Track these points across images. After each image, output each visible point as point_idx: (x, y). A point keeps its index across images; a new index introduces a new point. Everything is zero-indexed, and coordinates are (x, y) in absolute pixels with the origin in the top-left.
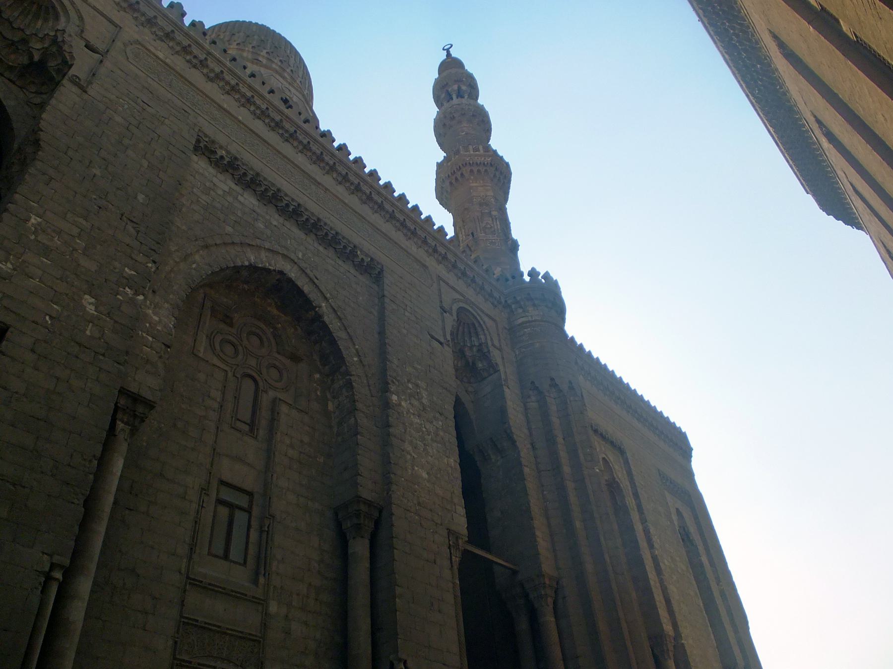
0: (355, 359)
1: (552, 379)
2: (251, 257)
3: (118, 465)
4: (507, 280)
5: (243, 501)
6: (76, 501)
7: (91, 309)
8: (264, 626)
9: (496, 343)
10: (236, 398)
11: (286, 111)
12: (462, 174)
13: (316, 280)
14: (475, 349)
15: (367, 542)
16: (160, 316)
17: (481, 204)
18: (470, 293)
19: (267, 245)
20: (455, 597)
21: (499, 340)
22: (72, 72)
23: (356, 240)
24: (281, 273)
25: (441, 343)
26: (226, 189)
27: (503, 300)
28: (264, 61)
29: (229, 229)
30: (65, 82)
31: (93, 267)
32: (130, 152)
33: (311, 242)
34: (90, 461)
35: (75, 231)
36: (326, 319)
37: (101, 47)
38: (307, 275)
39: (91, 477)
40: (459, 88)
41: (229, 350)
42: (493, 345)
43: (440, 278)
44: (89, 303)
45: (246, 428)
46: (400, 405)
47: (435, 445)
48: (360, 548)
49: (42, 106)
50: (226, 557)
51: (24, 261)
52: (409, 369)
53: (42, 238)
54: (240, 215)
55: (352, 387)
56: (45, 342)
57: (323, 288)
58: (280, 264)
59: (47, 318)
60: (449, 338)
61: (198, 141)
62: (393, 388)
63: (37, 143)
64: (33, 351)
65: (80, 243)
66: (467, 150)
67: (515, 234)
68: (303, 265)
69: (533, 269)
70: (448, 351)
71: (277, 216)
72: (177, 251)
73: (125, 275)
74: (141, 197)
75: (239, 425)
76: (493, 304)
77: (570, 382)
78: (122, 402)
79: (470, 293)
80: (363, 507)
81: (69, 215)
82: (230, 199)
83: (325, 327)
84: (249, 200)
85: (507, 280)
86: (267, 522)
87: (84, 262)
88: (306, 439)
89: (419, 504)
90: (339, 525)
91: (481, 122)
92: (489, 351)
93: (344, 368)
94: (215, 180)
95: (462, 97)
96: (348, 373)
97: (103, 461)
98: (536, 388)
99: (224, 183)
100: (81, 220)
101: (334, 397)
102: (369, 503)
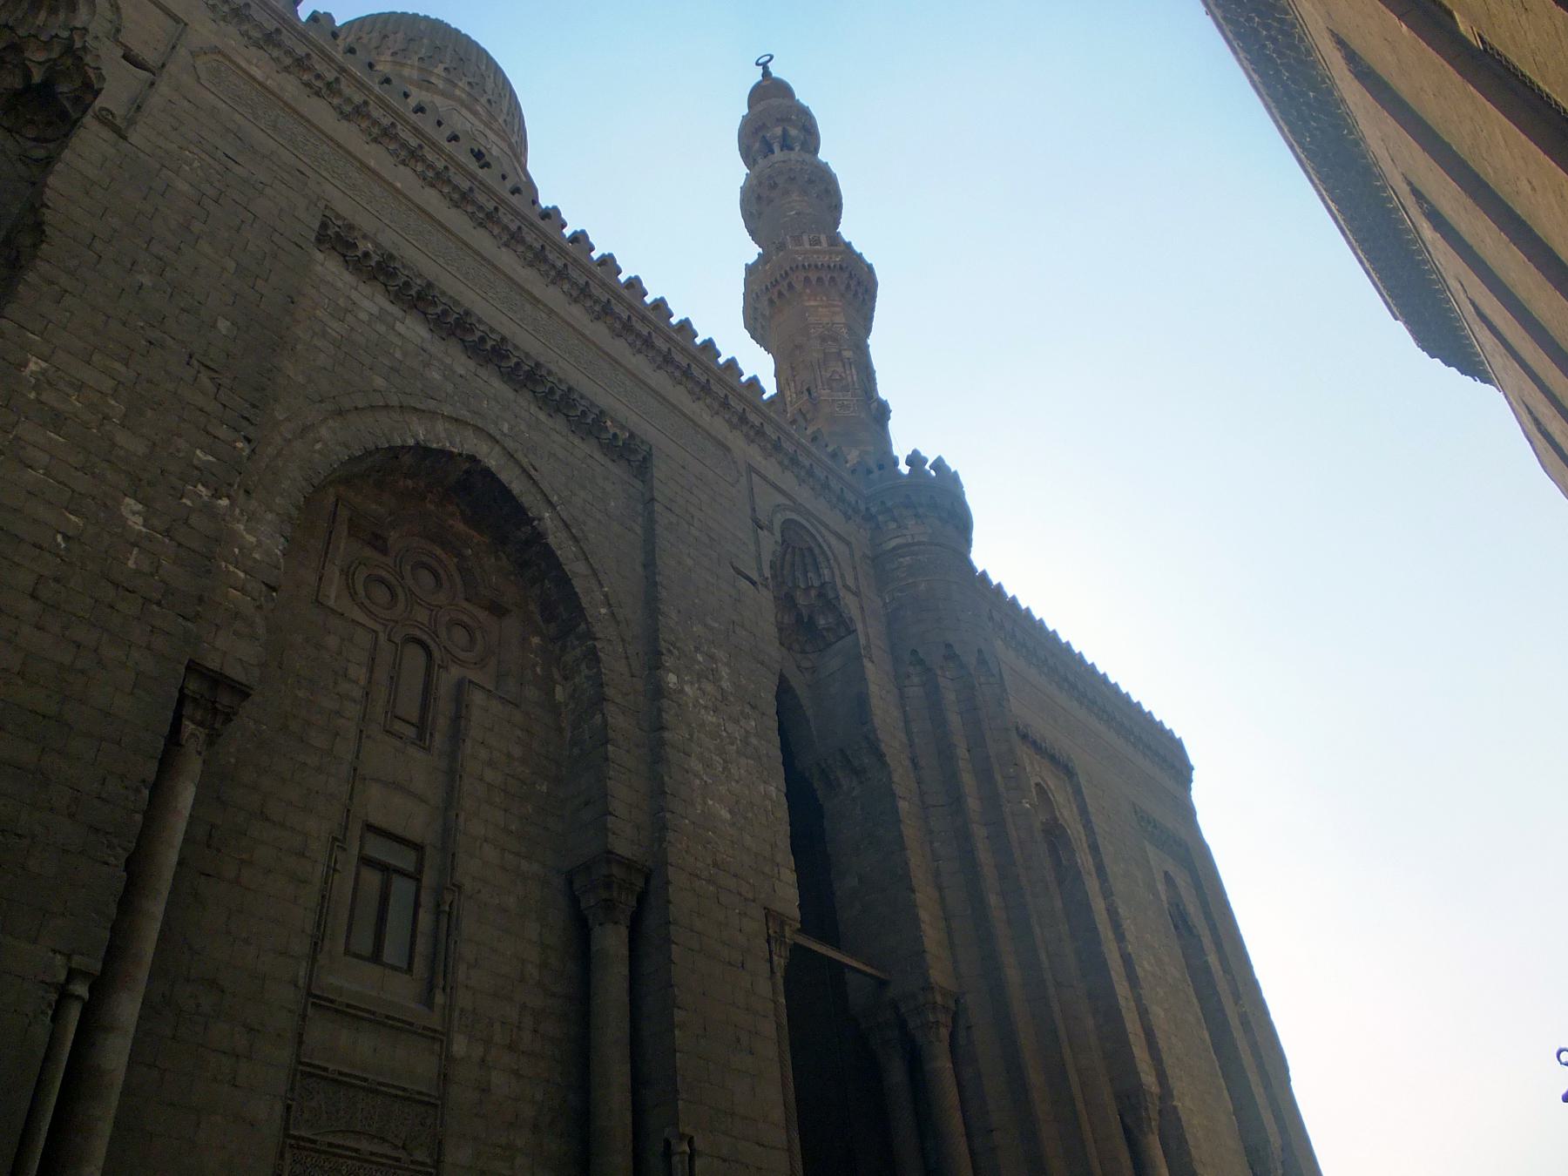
0: (603, 611)
1: (948, 646)
2: (419, 431)
3: (186, 796)
4: (869, 472)
5: (406, 860)
6: (112, 860)
7: (136, 523)
8: (444, 1078)
9: (851, 582)
10: (394, 680)
11: (481, 173)
12: (790, 286)
13: (533, 472)
14: (813, 593)
15: (624, 932)
16: (259, 536)
17: (823, 339)
18: (804, 495)
19: (447, 410)
20: (779, 1025)
21: (856, 579)
22: (98, 103)
23: (604, 400)
24: (472, 459)
25: (753, 583)
26: (375, 310)
27: (862, 508)
28: (441, 85)
29: (379, 382)
30: (88, 119)
31: (139, 447)
33: (524, 405)
34: (138, 791)
35: (108, 385)
36: (551, 540)
37: (150, 57)
38: (517, 462)
39: (138, 817)
40: (785, 132)
41: (381, 594)
42: (846, 586)
43: (751, 469)
44: (132, 513)
45: (411, 732)
46: (682, 691)
47: (743, 761)
48: (612, 941)
49: (47, 163)
50: (376, 957)
51: (17, 438)
52: (697, 629)
53: (49, 397)
54: (398, 355)
55: (598, 660)
56: (57, 580)
57: (545, 486)
58: (470, 444)
59: (59, 538)
60: (767, 573)
61: (324, 226)
62: (669, 662)
63: (38, 228)
64: (34, 596)
65: (117, 407)
66: (797, 240)
67: (884, 391)
68: (510, 444)
69: (915, 452)
70: (766, 598)
71: (463, 358)
72: (288, 419)
73: (195, 462)
74: (223, 325)
75: (398, 726)
76: (845, 514)
77: (980, 651)
78: (193, 686)
79: (804, 495)
80: (616, 870)
81: (96, 358)
82: (382, 328)
83: (549, 553)
84: (414, 330)
85: (869, 472)
86: (448, 897)
87: (122, 438)
88: (517, 751)
89: (715, 865)
90: (575, 901)
91: (823, 194)
92: (837, 597)
93: (583, 626)
94: (354, 295)
95: (791, 149)
97: (160, 789)
98: (921, 662)
99: (371, 301)
100: (117, 366)
101: (566, 678)
102: (628, 865)
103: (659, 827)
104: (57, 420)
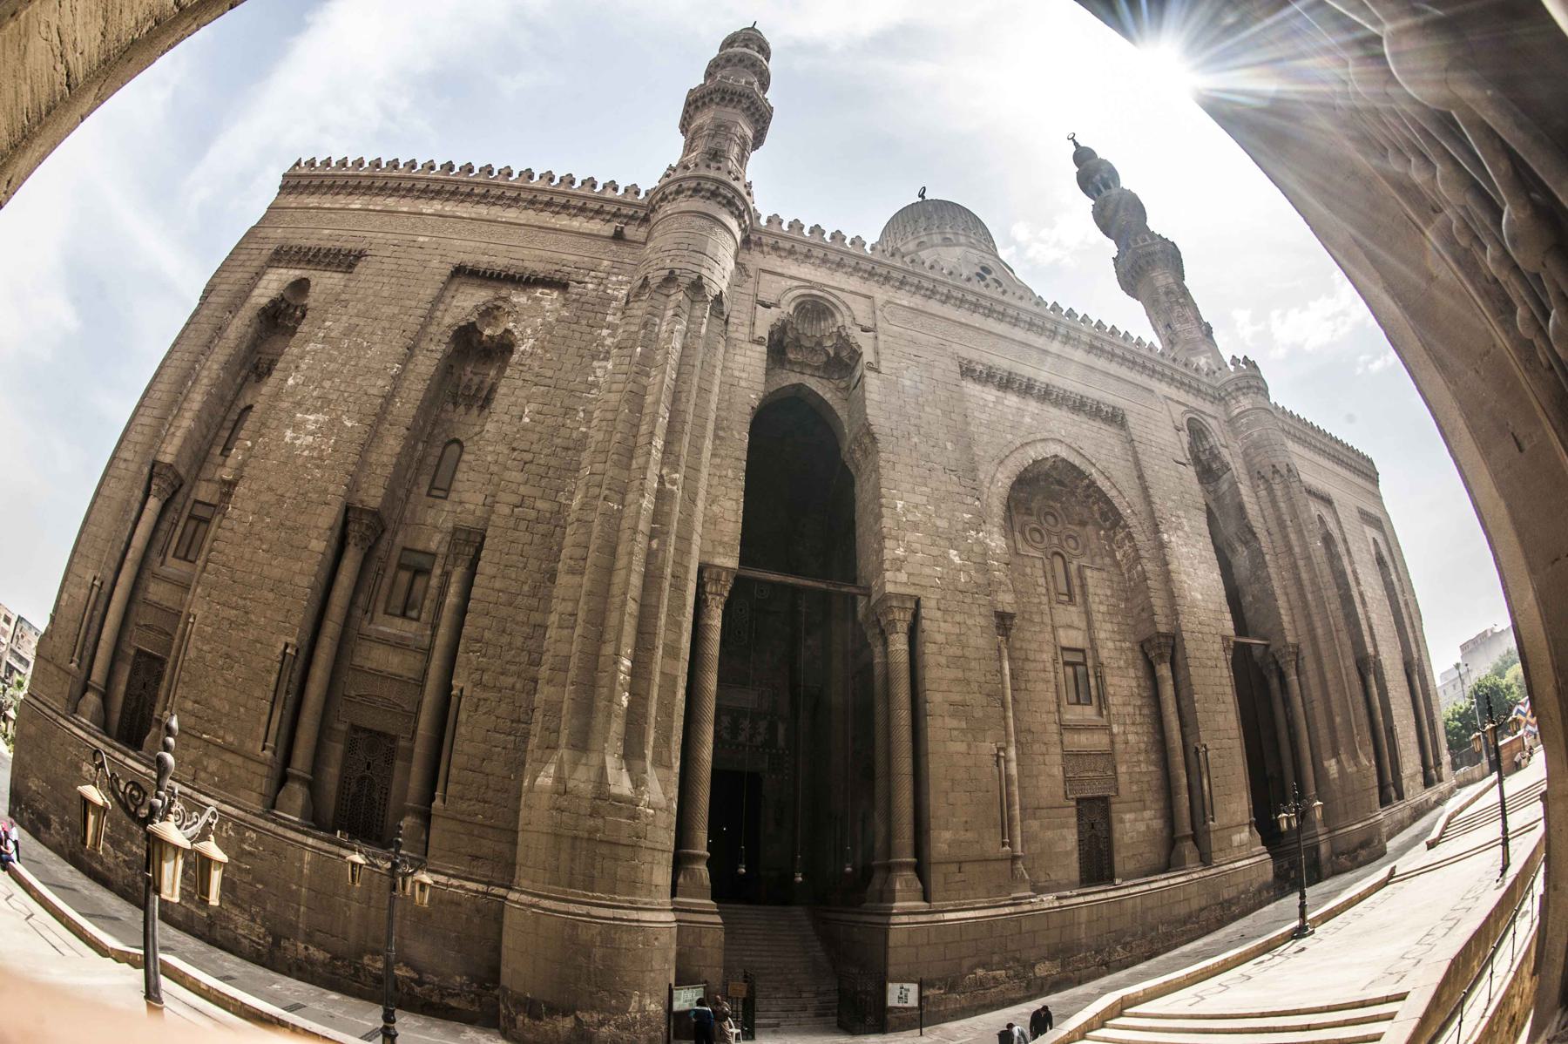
2: (1033, 453)
5: (1078, 658)
7: (957, 560)
8: (1112, 742)
16: (997, 542)
19: (1039, 436)
29: (1009, 437)
32: (927, 409)
41: (1037, 536)
45: (1066, 598)
50: (1078, 703)
52: (1170, 504)
53: (910, 517)
62: (1162, 528)
68: (1068, 441)
74: (949, 445)
80: (1162, 640)
83: (1099, 490)
87: (939, 523)
96: (1126, 526)
99: (990, 394)
102: (1165, 636)
103: (1174, 613)
104: (915, 526)
